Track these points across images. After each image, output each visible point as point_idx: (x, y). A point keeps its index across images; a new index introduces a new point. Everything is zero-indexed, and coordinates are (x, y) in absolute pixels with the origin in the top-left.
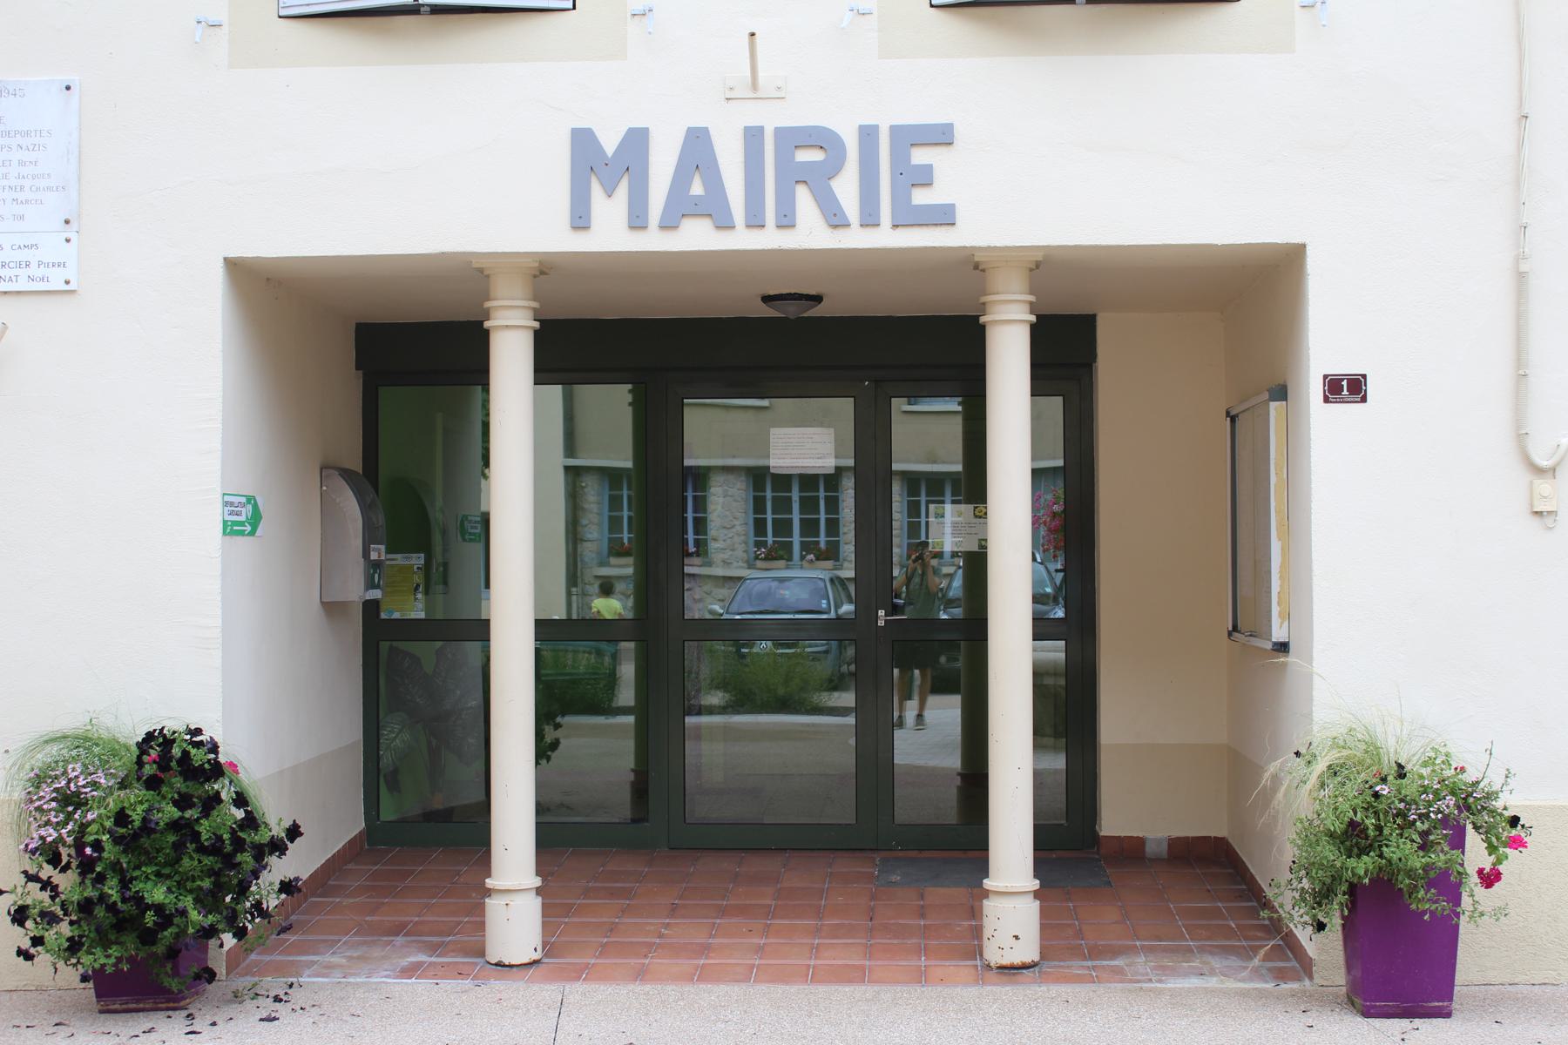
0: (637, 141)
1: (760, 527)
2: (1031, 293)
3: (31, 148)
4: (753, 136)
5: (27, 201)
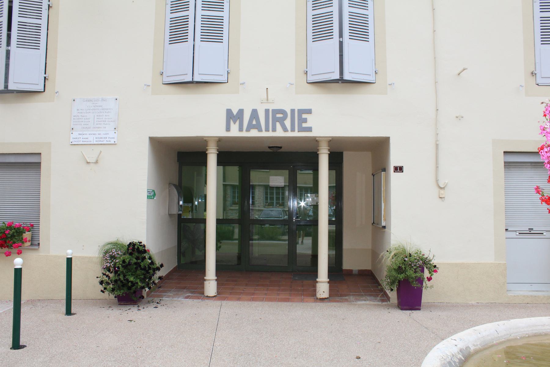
0: (241, 112)
4: (267, 111)
5: (107, 124)
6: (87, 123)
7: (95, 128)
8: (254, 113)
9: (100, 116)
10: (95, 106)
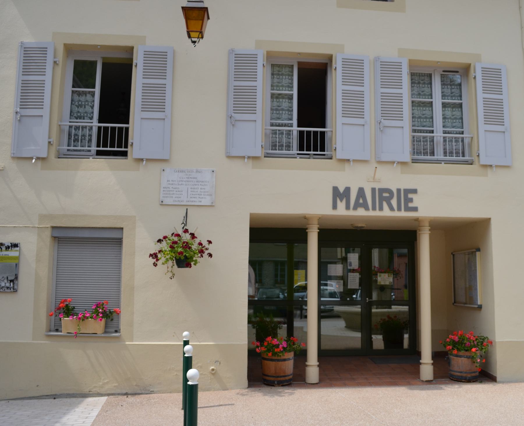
0: (348, 190)
1: (276, 276)
2: (318, 225)
3: (204, 185)
4: (373, 190)
5: (202, 198)
6: (180, 196)
7: (188, 201)
8: (361, 192)
9: (194, 188)
10: (188, 178)
